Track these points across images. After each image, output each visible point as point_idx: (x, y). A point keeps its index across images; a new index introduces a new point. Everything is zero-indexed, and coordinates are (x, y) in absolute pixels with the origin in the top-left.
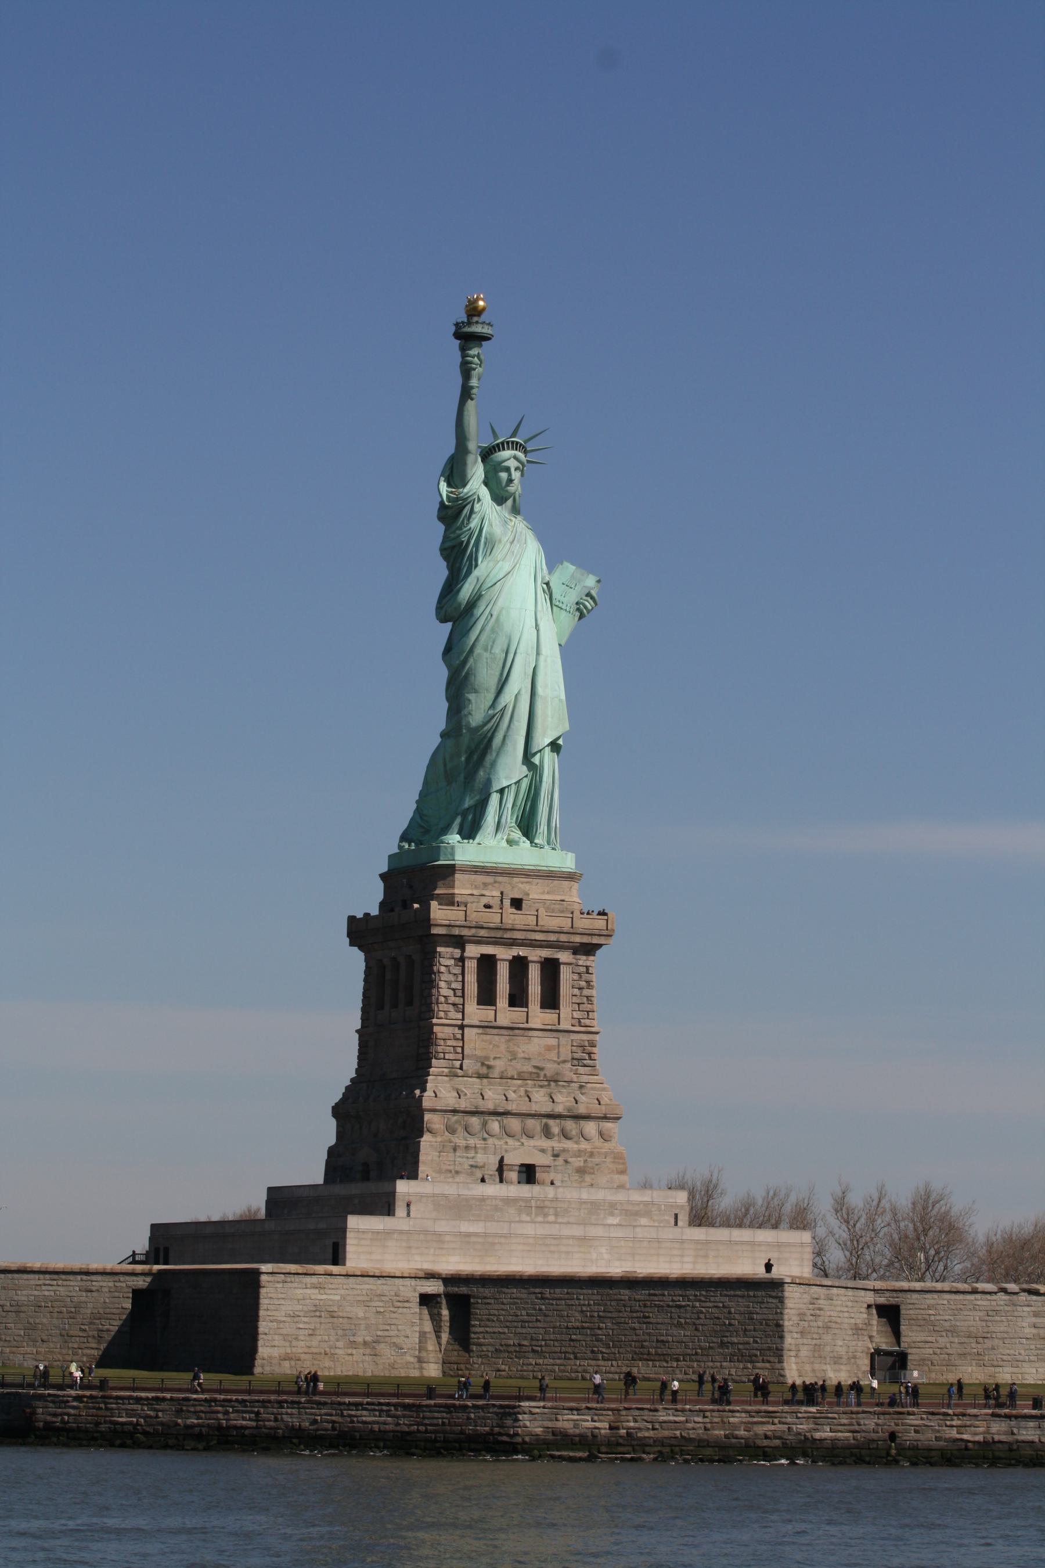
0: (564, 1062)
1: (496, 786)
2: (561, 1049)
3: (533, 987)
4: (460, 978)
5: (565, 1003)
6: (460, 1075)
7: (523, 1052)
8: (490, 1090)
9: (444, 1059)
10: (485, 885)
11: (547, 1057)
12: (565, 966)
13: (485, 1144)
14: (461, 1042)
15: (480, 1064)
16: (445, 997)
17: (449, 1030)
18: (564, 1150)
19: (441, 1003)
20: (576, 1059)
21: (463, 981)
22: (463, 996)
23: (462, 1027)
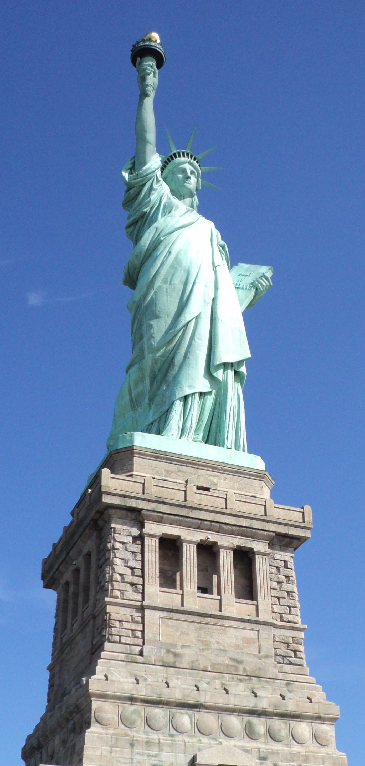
0: (267, 657)
1: (180, 394)
2: (261, 643)
3: (226, 573)
4: (139, 557)
5: (263, 594)
6: (140, 661)
7: (218, 643)
8: (177, 679)
9: (120, 642)
10: (168, 472)
11: (246, 650)
12: (261, 556)
13: (172, 740)
14: (141, 625)
15: (165, 650)
16: (120, 575)
17: (126, 613)
18: (273, 752)
19: (117, 581)
20: (280, 656)
21: (143, 561)
22: (143, 577)
23: (142, 609)
